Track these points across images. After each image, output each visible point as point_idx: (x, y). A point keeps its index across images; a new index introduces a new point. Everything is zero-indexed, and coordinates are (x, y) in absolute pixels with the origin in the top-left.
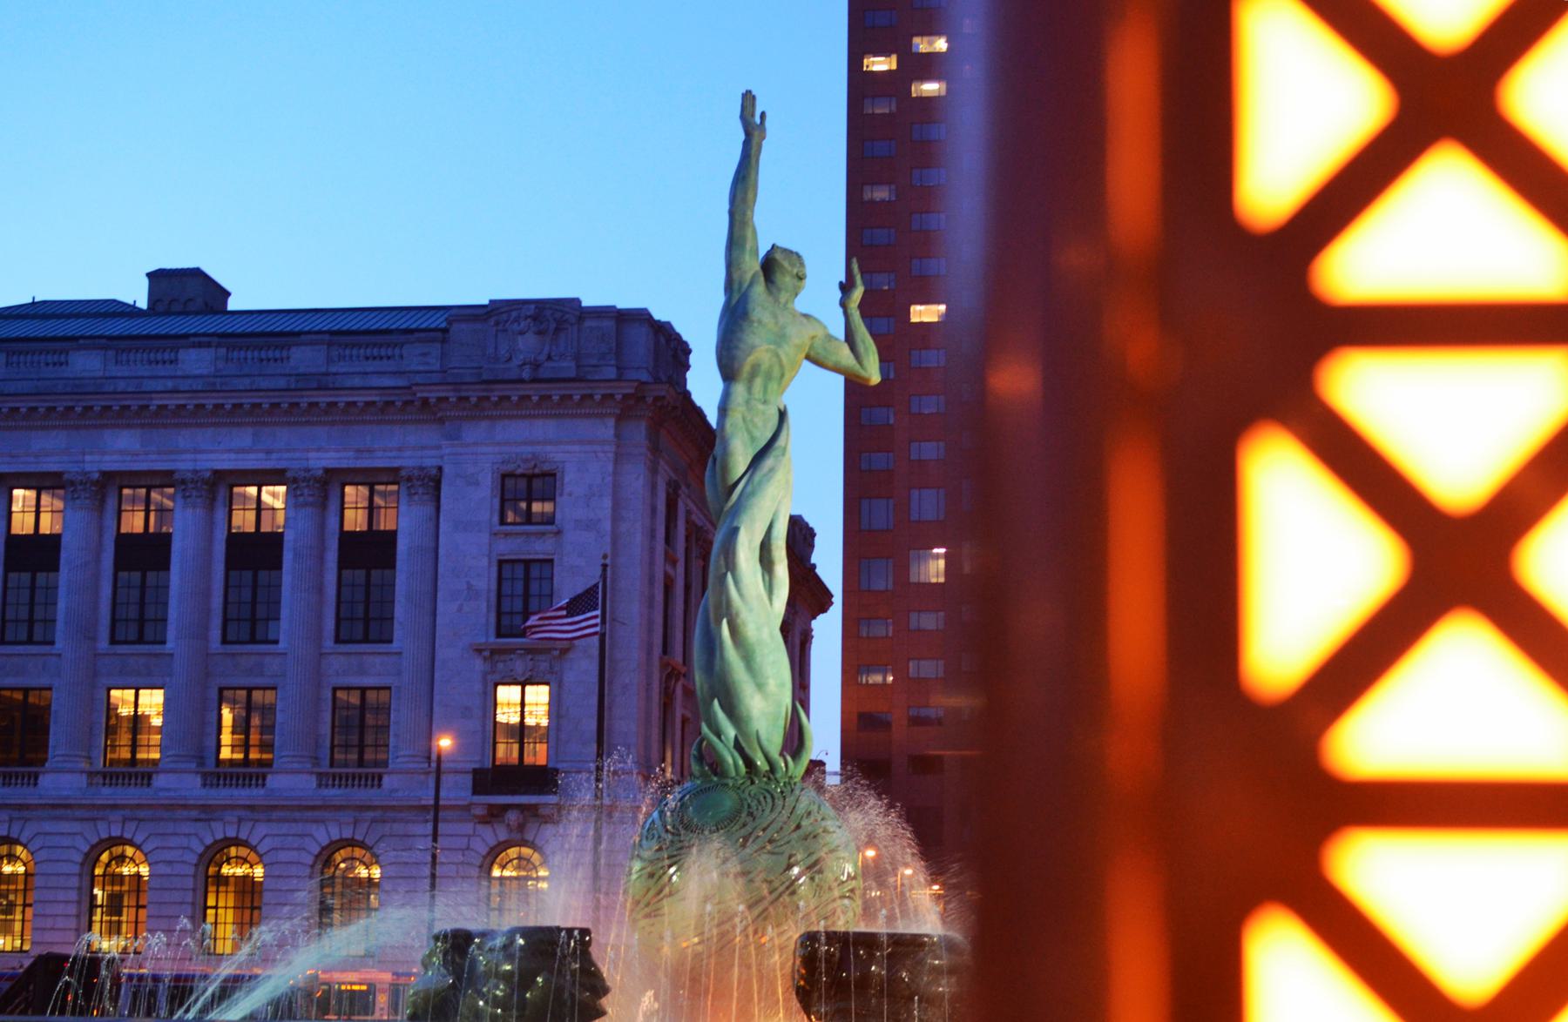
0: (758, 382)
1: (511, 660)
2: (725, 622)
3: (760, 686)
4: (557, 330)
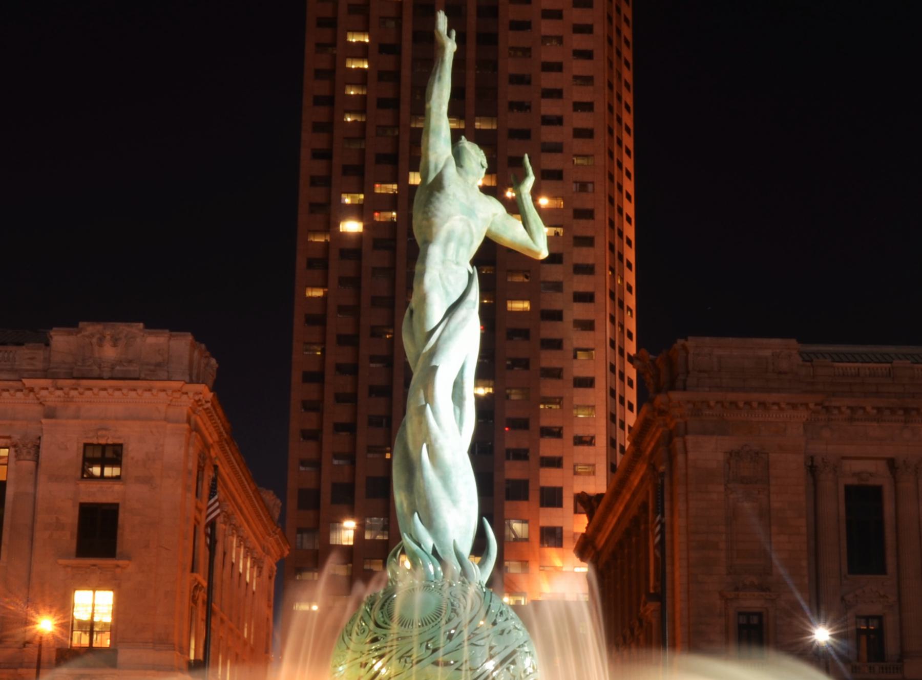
0: (452, 246)
2: (425, 446)
3: (455, 502)
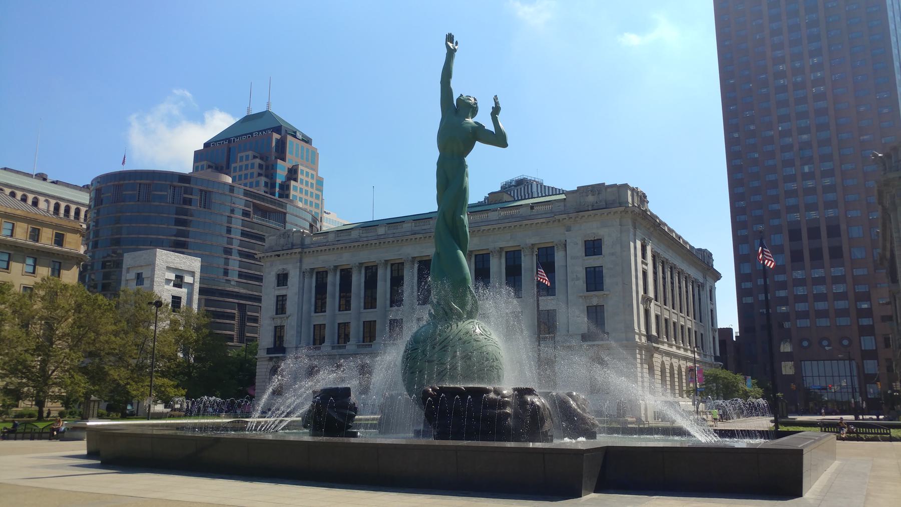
4: (599, 194)
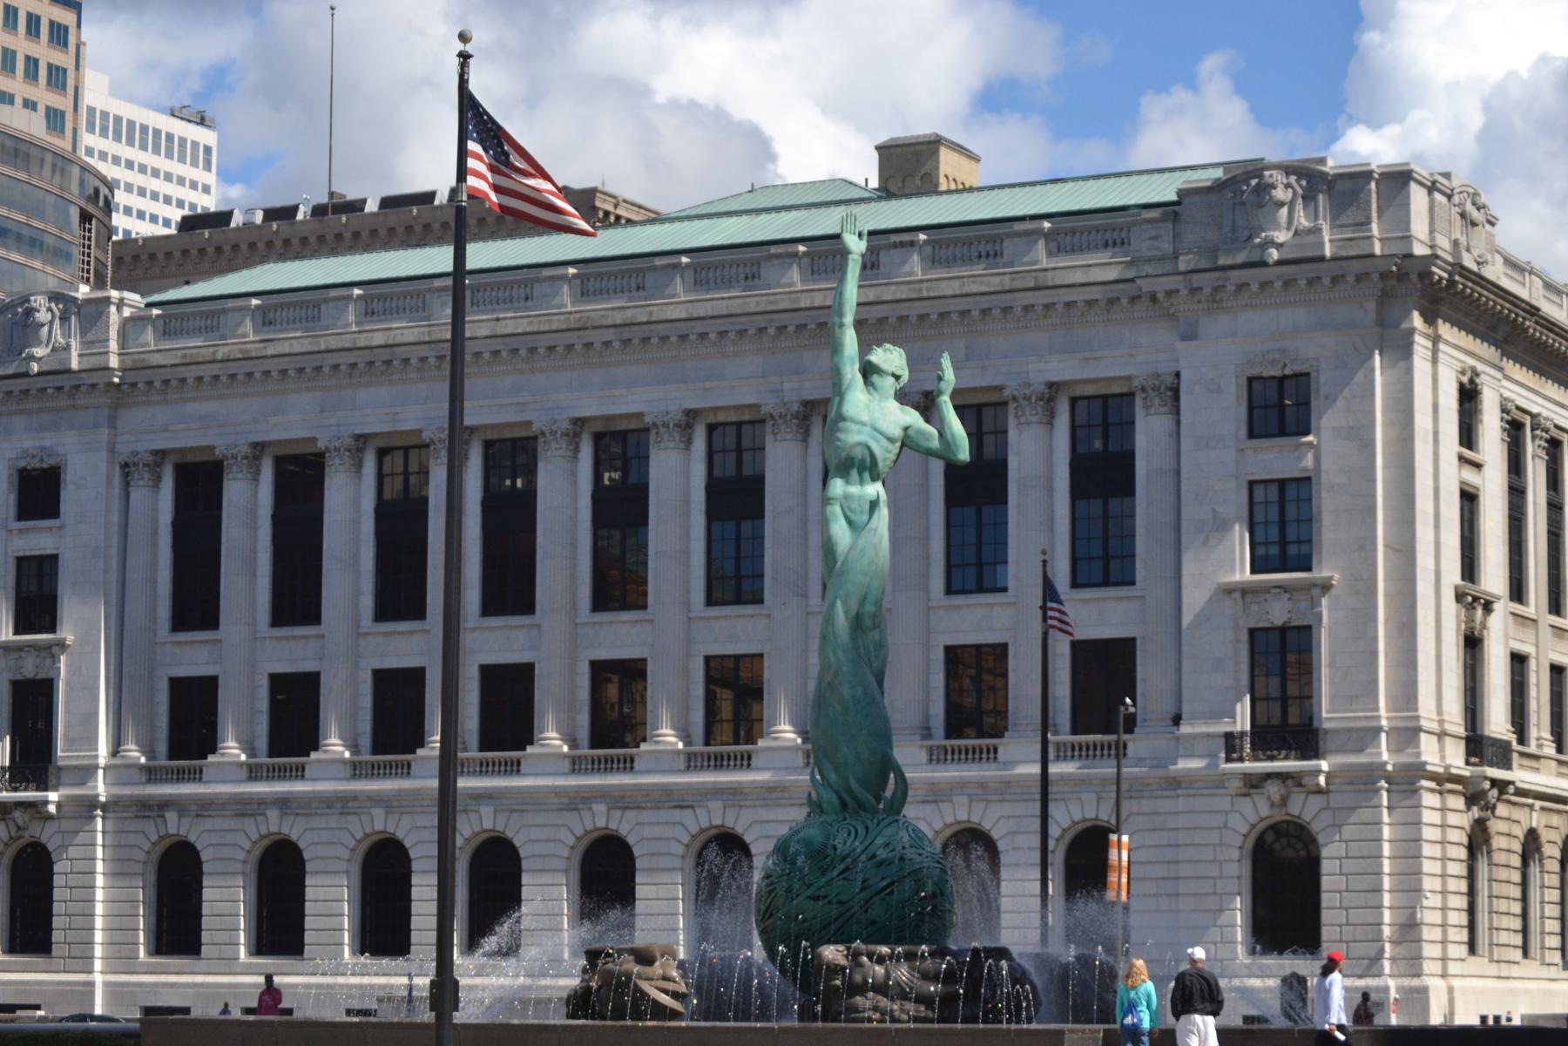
1: (1266, 600)
